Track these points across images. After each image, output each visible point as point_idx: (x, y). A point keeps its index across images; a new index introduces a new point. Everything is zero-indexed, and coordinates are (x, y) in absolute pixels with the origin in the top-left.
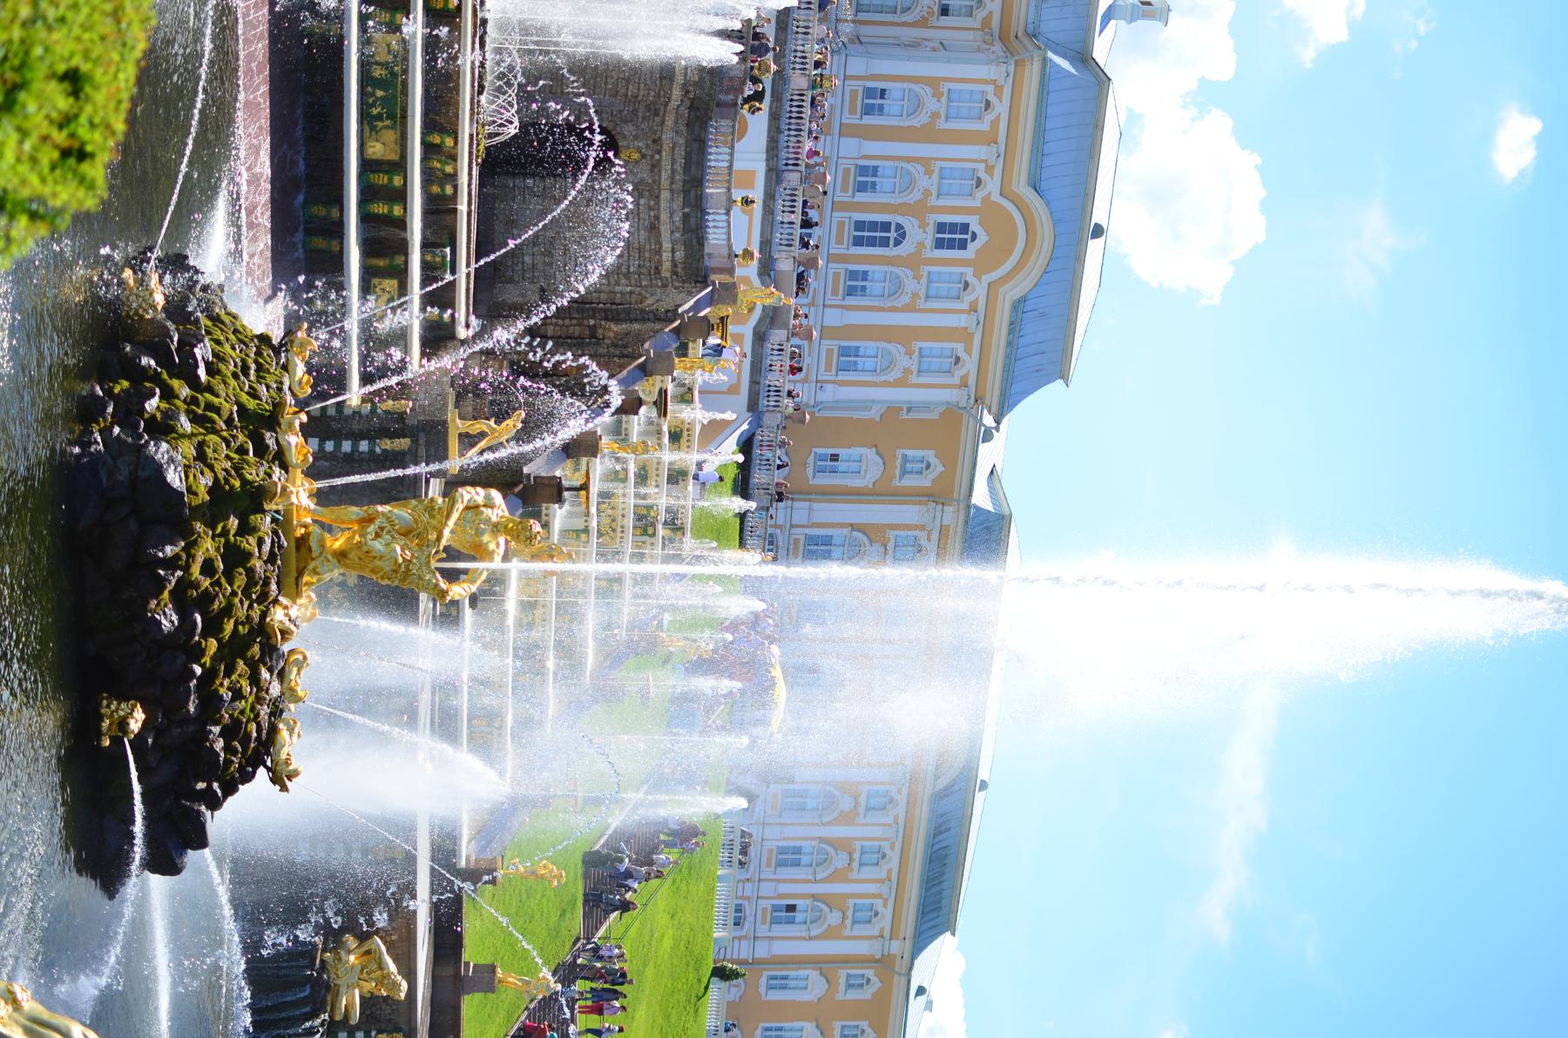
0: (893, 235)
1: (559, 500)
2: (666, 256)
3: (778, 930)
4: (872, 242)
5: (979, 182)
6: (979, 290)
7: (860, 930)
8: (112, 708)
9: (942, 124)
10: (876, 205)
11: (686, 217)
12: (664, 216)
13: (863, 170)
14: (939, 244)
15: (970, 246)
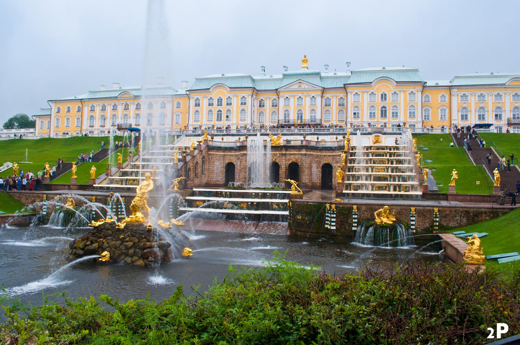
0: (384, 109)
4: (386, 113)
5: (372, 93)
10: (378, 113)
11: (338, 150)
12: (338, 154)
13: (370, 116)
14: (385, 99)
15: (386, 93)
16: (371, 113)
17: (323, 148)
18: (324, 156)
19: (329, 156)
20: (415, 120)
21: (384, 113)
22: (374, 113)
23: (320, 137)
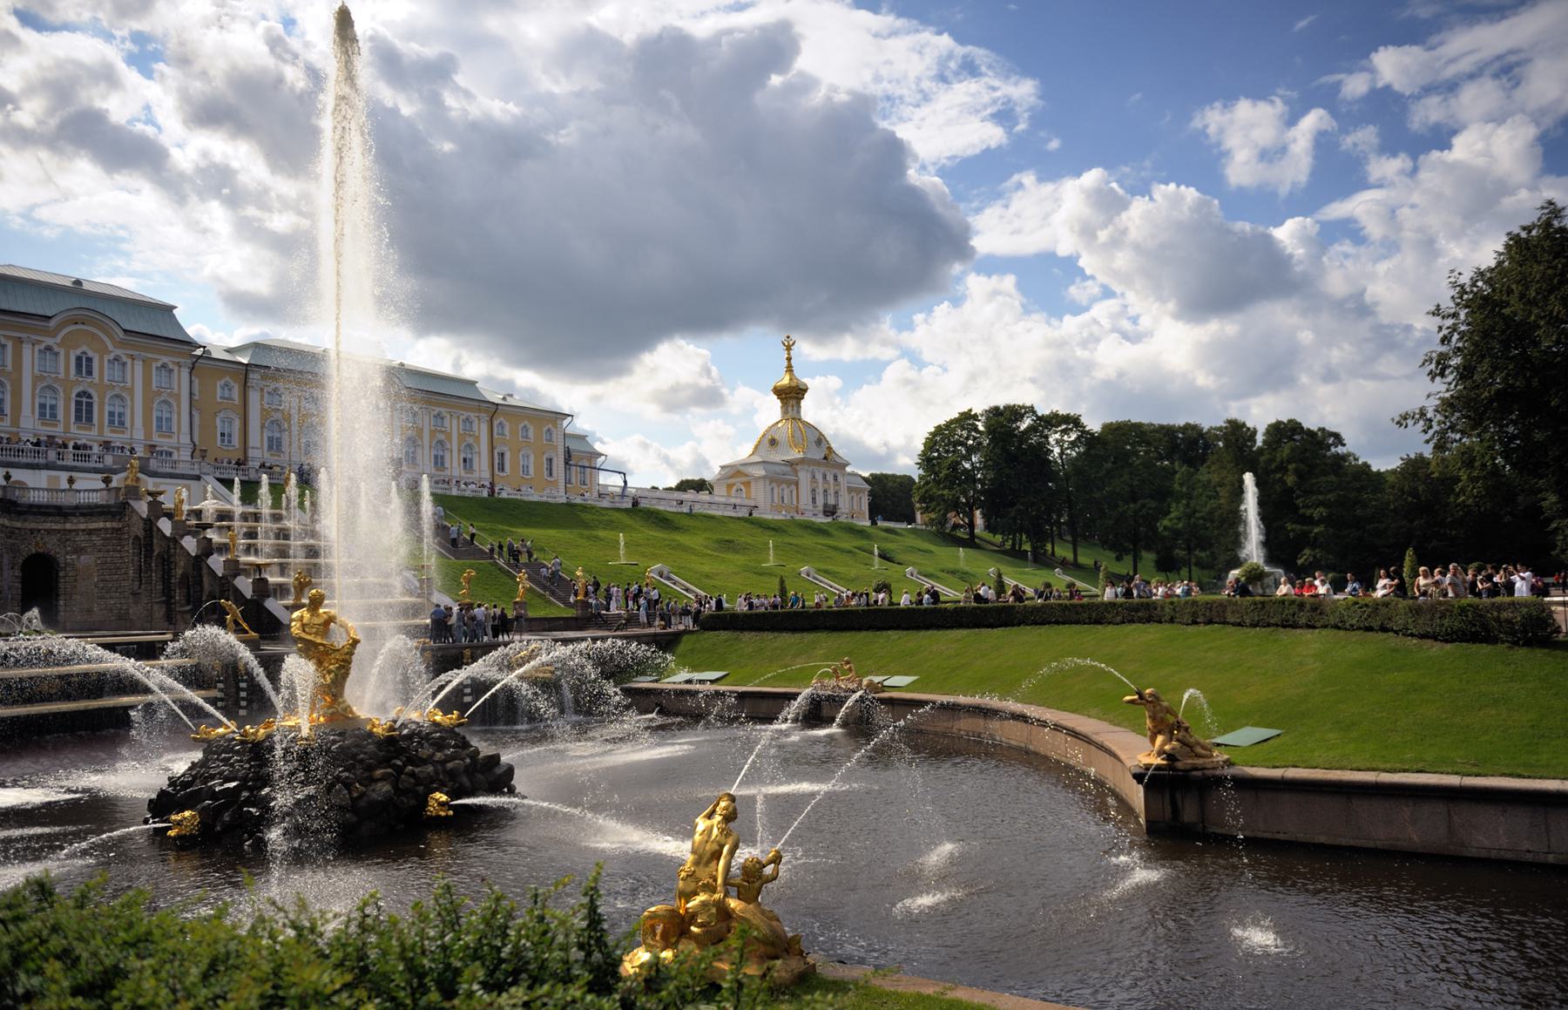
1: (265, 581)
2: (108, 525)
3: (476, 466)
6: (119, 352)
7: (475, 427)
8: (432, 809)
9: (9, 368)
11: (82, 515)
12: (82, 526)
13: (42, 415)
14: (90, 373)
15: (90, 354)
16: (42, 406)
17: (31, 506)
18: (32, 531)
19: (49, 532)
20: (174, 441)
21: (84, 411)
22: (53, 407)
23: (12, 472)
